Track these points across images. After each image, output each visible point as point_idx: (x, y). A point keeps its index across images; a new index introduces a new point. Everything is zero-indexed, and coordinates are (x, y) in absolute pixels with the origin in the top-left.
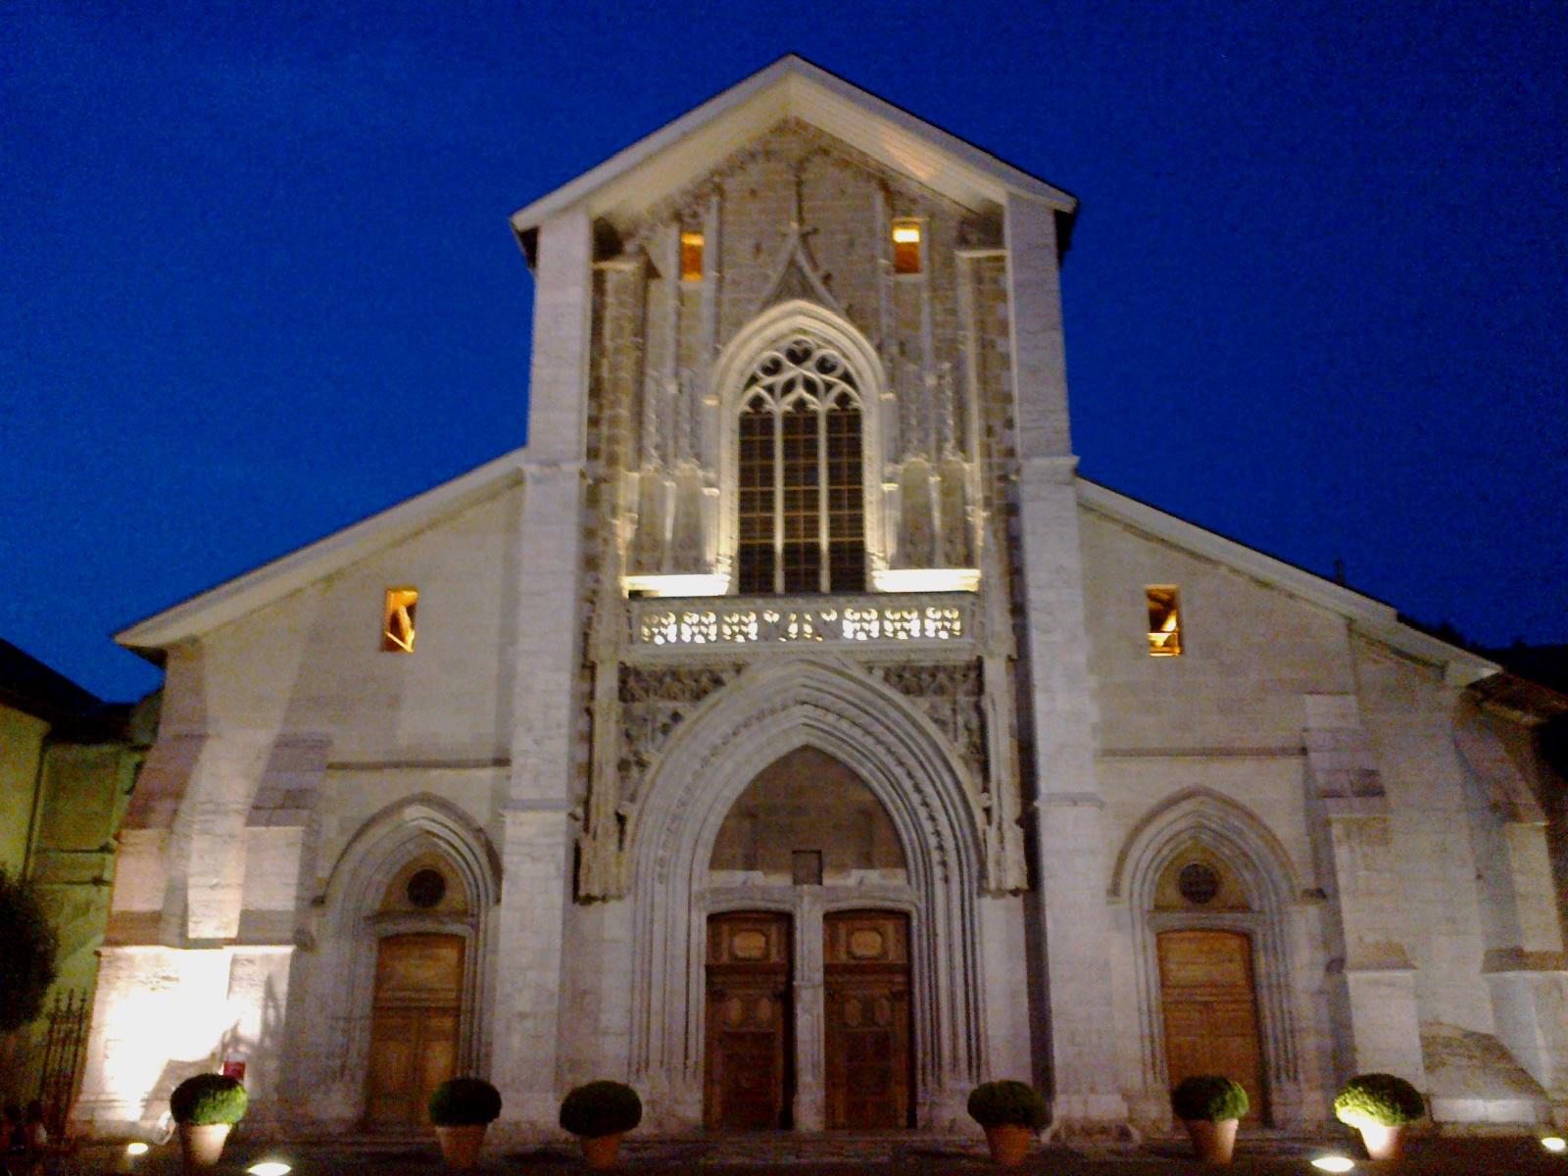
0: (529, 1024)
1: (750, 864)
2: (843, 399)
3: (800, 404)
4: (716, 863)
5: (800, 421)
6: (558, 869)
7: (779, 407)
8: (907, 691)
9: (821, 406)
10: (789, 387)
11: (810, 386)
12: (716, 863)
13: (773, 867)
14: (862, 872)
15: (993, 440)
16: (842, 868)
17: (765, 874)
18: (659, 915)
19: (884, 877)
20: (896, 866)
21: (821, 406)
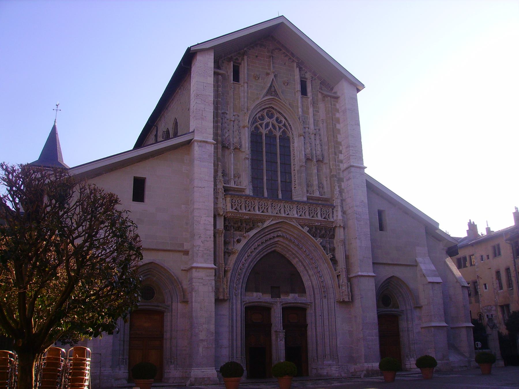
0: (205, 343)
1: (257, 291)
2: (284, 132)
3: (270, 131)
4: (247, 289)
5: (271, 136)
6: (213, 288)
7: (264, 131)
8: (313, 236)
9: (278, 134)
10: (267, 125)
11: (273, 126)
12: (247, 289)
13: (263, 293)
14: (293, 295)
15: (336, 157)
16: (287, 293)
18: (234, 307)
19: (299, 296)
21: (278, 134)
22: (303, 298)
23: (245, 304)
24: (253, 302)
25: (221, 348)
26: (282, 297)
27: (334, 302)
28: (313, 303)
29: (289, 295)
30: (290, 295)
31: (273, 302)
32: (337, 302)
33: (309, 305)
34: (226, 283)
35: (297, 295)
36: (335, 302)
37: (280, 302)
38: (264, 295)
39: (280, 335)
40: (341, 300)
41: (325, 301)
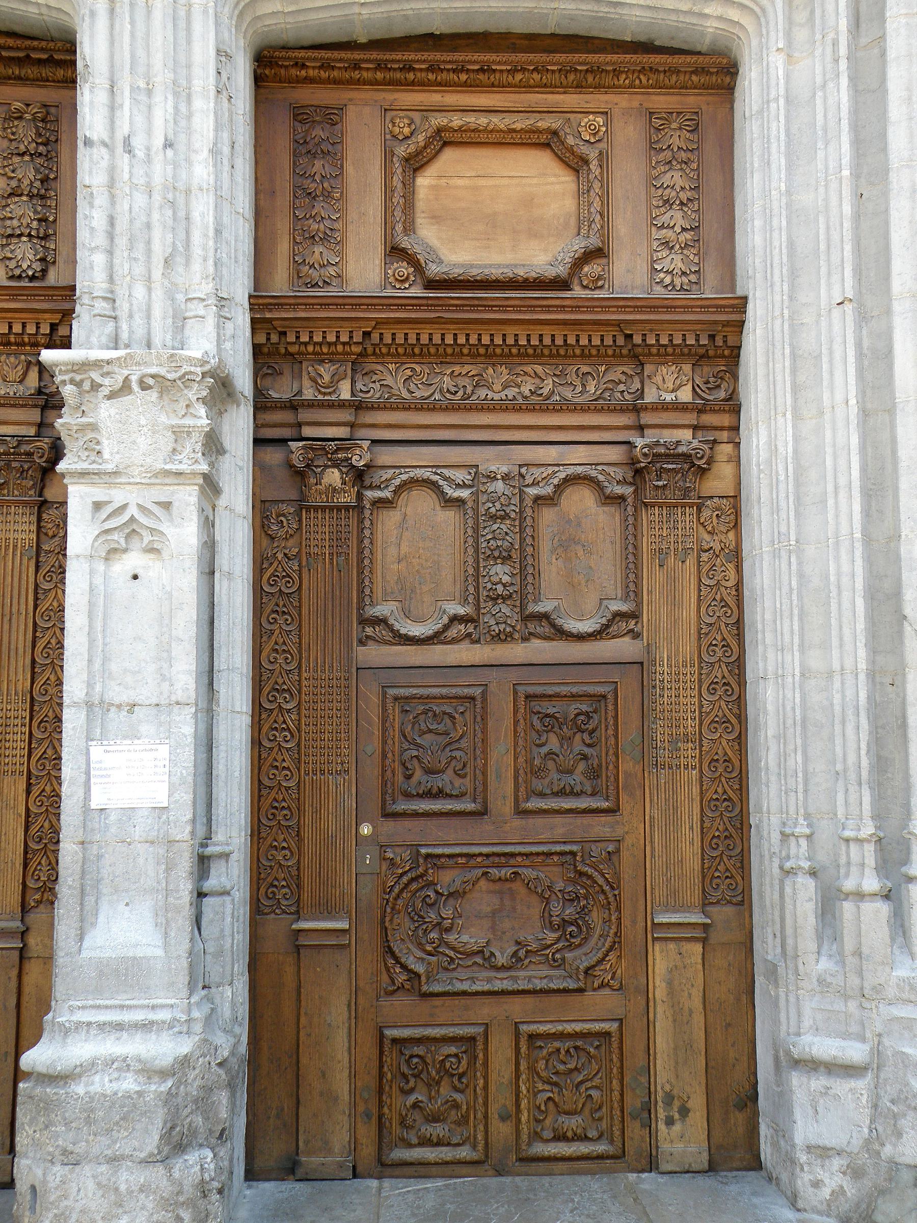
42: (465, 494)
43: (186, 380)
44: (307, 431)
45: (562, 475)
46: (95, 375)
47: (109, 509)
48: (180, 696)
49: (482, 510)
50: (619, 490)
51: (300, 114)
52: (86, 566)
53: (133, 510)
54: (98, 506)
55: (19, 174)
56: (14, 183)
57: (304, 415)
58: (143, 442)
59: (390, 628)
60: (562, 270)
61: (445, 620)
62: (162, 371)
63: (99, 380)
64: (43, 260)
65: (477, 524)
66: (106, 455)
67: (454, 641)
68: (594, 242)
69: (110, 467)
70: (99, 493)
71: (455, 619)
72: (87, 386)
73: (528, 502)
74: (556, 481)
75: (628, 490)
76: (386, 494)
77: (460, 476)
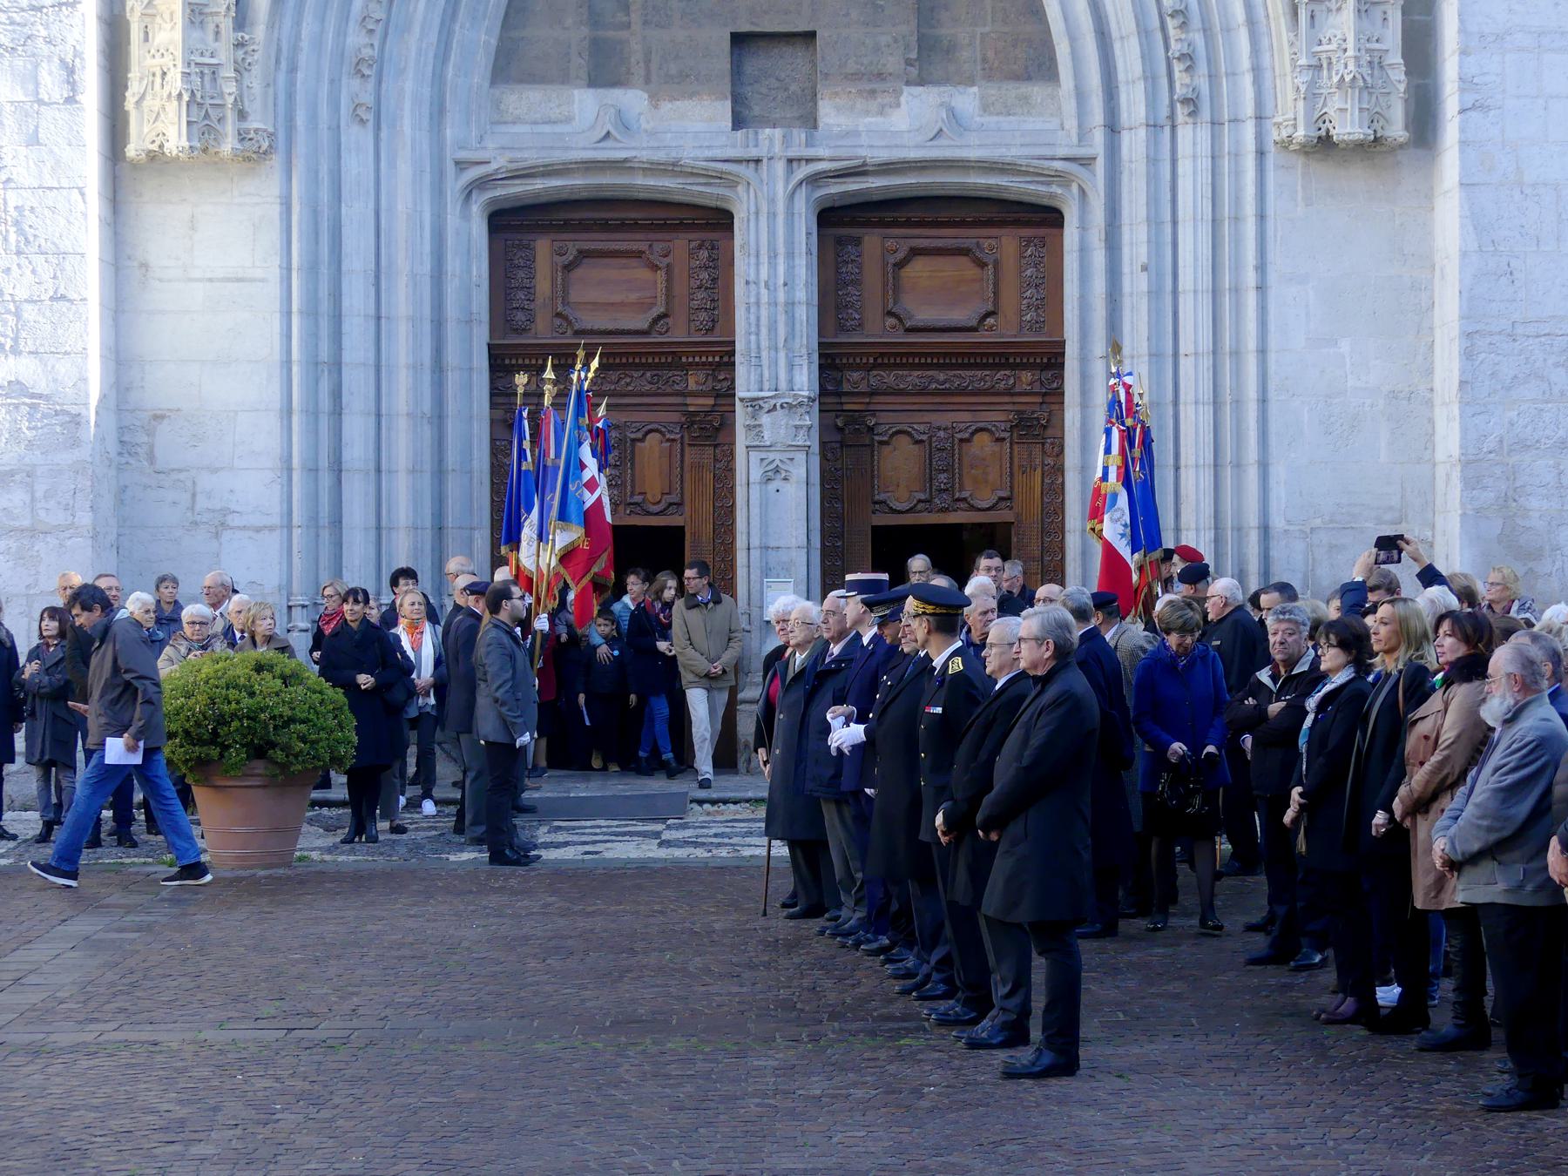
17: (655, 99)
19: (985, 108)
20: (1026, 77)
22: (1033, 123)
23: (469, 191)
24: (549, 171)
25: (217, 535)
26: (830, 114)
27: (1261, 153)
28: (1100, 166)
29: (897, 93)
30: (903, 99)
31: (719, 166)
32: (1284, 145)
33: (1062, 178)
34: (227, 24)
35: (967, 100)
36: (1271, 149)
37: (790, 161)
38: (666, 106)
39: (766, 434)
40: (1300, 134)
41: (1192, 139)
42: (924, 437)
43: (801, 404)
44: (846, 407)
45: (974, 428)
46: (761, 402)
47: (766, 462)
48: (800, 544)
49: (934, 445)
50: (1003, 435)
51: (840, 242)
52: (758, 487)
53: (777, 462)
54: (762, 460)
55: (701, 277)
56: (698, 282)
57: (844, 400)
58: (782, 432)
59: (888, 505)
60: (974, 323)
61: (915, 502)
62: (790, 401)
63: (763, 405)
64: (713, 320)
65: (931, 453)
66: (766, 438)
67: (920, 512)
68: (990, 308)
69: (768, 443)
70: (763, 455)
71: (920, 501)
72: (757, 407)
73: (956, 441)
74: (970, 431)
75: (1006, 435)
76: (885, 438)
77: (921, 428)
